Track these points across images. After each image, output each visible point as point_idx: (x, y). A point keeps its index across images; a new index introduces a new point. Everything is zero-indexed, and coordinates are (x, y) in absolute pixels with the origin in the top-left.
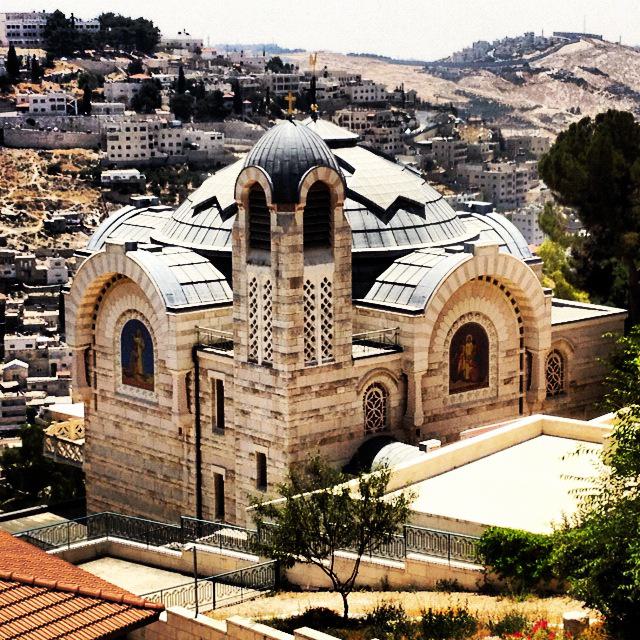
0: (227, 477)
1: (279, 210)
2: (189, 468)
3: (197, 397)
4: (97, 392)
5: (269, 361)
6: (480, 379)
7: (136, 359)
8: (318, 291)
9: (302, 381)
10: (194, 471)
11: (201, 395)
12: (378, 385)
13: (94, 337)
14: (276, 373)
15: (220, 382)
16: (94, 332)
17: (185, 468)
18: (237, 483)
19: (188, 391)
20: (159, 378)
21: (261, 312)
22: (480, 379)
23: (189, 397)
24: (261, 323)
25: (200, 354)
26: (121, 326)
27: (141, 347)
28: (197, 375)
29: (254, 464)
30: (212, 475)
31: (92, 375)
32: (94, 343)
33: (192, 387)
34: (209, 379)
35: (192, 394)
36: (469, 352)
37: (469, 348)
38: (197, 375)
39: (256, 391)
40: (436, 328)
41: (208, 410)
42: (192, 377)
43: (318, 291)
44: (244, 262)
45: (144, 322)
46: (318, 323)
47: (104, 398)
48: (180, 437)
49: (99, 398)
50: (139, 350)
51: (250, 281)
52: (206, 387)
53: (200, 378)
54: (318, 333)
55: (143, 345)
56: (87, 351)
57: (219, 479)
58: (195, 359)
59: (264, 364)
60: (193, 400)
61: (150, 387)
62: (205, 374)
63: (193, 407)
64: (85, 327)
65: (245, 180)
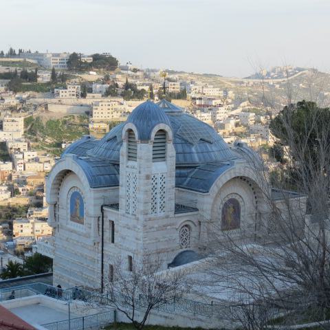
1: (141, 143)
2: (98, 260)
3: (103, 228)
6: (236, 225)
7: (76, 209)
8: (159, 181)
9: (150, 224)
10: (100, 262)
11: (104, 227)
12: (186, 226)
14: (138, 219)
15: (113, 222)
19: (98, 225)
20: (86, 220)
21: (132, 190)
22: (236, 225)
23: (98, 227)
24: (132, 195)
25: (104, 208)
26: (71, 193)
28: (103, 217)
29: (127, 260)
31: (57, 216)
33: (101, 223)
35: (101, 226)
36: (231, 212)
37: (231, 210)
38: (103, 217)
39: (129, 228)
40: (215, 200)
41: (108, 235)
42: (101, 219)
43: (159, 181)
45: (80, 193)
46: (158, 196)
52: (107, 225)
53: (104, 219)
54: (158, 200)
56: (55, 205)
57: (111, 267)
58: (102, 210)
60: (101, 229)
61: (83, 223)
63: (101, 234)
64: (56, 193)
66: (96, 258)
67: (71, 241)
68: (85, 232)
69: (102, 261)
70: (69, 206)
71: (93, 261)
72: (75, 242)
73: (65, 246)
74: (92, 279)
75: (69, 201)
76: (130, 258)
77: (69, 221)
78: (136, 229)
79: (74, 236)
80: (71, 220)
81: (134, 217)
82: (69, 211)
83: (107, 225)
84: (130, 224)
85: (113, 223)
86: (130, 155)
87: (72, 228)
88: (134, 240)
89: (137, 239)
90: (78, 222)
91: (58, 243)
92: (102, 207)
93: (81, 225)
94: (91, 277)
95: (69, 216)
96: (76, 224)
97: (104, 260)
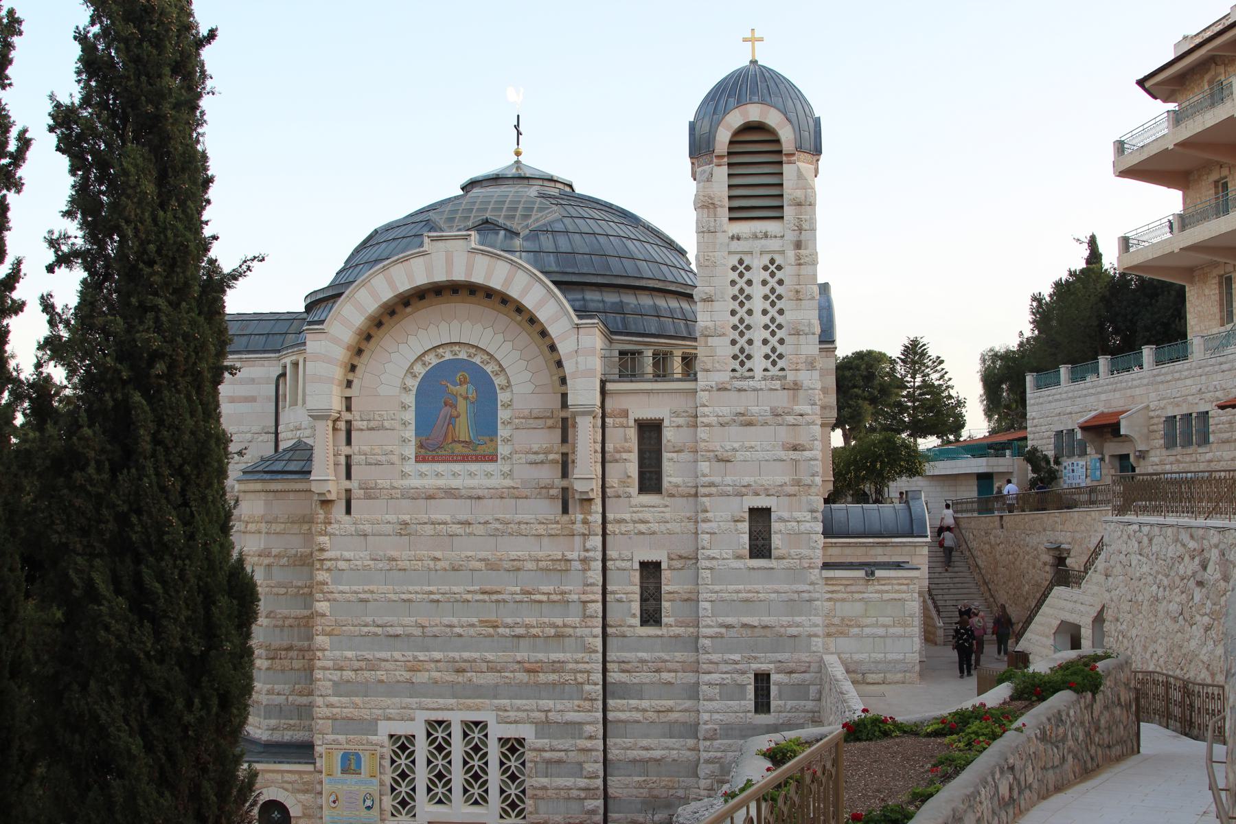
0: (670, 559)
2: (584, 561)
4: (353, 485)
5: (774, 371)
7: (452, 419)
10: (600, 564)
11: (609, 447)
13: (348, 399)
14: (796, 387)
16: (348, 393)
17: (577, 565)
18: (703, 563)
25: (609, 386)
26: (420, 370)
27: (466, 398)
30: (637, 566)
32: (349, 409)
33: (599, 438)
34: (632, 423)
44: (722, 238)
47: (370, 493)
48: (566, 518)
49: (357, 493)
50: (462, 405)
51: (734, 261)
55: (472, 395)
57: (650, 570)
58: (603, 392)
59: (764, 379)
60: (599, 456)
61: (492, 458)
62: (625, 414)
65: (736, 119)
66: (569, 555)
67: (428, 529)
68: (508, 482)
69: (604, 560)
70: (410, 416)
71: (561, 567)
72: (457, 529)
73: (395, 554)
74: (552, 632)
75: (410, 399)
76: (760, 517)
77: (411, 467)
78: (790, 419)
79: (444, 511)
80: (420, 459)
81: (777, 384)
82: (410, 433)
83: (626, 440)
84: (755, 409)
85: (650, 431)
86: (736, 203)
87: (430, 483)
88: (782, 454)
89: (795, 448)
90: (464, 459)
91: (347, 554)
92: (603, 383)
93: (489, 467)
94: (542, 626)
95: (410, 451)
96: (457, 467)
97: (611, 553)
